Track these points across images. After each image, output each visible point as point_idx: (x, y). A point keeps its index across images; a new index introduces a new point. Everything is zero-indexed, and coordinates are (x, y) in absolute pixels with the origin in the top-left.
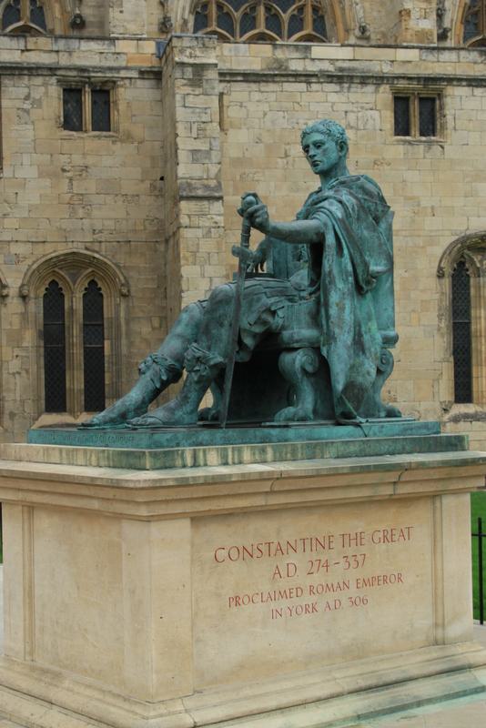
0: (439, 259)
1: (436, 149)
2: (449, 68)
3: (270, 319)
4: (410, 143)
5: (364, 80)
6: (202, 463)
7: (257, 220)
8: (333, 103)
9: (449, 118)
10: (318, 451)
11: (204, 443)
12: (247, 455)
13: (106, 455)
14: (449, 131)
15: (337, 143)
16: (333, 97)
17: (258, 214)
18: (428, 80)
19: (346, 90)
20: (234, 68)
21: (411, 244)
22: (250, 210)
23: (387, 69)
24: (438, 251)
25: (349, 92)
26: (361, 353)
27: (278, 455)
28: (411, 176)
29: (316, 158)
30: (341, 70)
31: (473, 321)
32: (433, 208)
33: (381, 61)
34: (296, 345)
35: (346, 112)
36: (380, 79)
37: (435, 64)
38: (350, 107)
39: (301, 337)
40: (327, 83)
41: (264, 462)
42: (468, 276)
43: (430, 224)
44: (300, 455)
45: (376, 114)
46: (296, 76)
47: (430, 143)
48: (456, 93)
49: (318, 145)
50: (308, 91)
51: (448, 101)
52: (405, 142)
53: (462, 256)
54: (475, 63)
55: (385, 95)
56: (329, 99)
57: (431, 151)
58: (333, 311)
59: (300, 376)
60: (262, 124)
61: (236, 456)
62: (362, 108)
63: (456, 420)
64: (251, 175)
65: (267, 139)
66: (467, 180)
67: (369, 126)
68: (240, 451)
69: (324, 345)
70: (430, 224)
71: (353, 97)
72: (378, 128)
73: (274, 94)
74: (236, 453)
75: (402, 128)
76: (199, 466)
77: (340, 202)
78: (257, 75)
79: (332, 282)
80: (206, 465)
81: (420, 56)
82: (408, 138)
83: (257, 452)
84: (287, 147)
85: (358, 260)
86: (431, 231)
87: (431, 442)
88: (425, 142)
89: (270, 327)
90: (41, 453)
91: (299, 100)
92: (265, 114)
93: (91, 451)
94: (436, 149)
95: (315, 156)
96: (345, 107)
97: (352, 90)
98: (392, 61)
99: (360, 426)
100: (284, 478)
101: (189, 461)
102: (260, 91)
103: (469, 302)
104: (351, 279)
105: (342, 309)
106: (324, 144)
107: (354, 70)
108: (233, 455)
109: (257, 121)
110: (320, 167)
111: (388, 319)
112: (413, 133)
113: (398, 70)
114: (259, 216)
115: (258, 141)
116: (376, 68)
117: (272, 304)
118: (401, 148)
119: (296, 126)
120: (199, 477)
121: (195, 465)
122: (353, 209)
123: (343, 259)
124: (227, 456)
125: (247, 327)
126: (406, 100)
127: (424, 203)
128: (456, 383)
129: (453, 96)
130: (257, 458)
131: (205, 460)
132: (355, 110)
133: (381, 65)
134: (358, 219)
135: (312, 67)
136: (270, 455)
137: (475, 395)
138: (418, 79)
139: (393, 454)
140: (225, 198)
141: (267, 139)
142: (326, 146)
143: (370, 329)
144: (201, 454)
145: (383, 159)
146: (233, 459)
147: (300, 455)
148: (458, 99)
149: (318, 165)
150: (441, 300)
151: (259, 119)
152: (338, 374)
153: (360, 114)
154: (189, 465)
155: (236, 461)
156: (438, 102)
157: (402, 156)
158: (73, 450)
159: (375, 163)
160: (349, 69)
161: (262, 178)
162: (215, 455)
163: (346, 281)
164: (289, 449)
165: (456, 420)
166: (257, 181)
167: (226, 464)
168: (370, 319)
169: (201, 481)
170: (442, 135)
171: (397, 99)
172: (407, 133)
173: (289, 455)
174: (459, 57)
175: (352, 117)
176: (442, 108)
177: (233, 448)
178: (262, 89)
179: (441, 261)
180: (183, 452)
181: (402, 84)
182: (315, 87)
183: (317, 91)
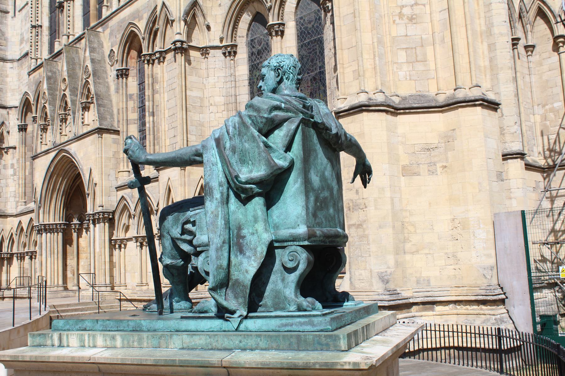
6: (65, 345)
10: (162, 341)
11: (88, 329)
12: (100, 341)
26: (238, 254)
27: (126, 342)
39: (200, 242)
44: (145, 344)
61: (91, 341)
68: (94, 337)
74: (91, 338)
76: (63, 346)
80: (68, 346)
83: (108, 339)
87: (292, 340)
101: (56, 343)
108: (89, 340)
111: (298, 218)
117: (191, 217)
120: (26, 356)
121: (60, 346)
122: (234, 127)
124: (85, 340)
125: (179, 236)
130: (108, 343)
131: (68, 342)
134: (239, 135)
136: (119, 343)
139: (244, 349)
143: (257, 230)
144: (64, 338)
146: (89, 342)
147: (145, 344)
154: (56, 345)
155: (91, 345)
162: (75, 339)
164: (136, 338)
168: (256, 220)
169: (28, 359)
173: (136, 344)
177: (89, 334)
180: (52, 336)
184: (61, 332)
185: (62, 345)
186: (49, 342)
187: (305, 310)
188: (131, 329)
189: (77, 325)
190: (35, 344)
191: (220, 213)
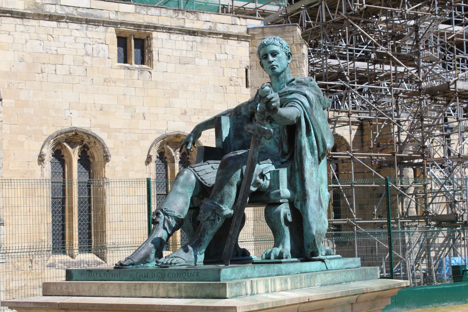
0: (148, 150)
2: (154, 19)
3: (261, 181)
4: (128, 68)
7: (273, 104)
8: (76, 37)
9: (155, 53)
13: (177, 287)
14: (154, 62)
15: (286, 54)
17: (273, 100)
20: (4, 6)
22: (269, 97)
23: (113, 17)
24: (148, 144)
29: (273, 63)
33: (109, 10)
34: (281, 201)
36: (107, 23)
37: (146, 16)
40: (71, 22)
41: (286, 290)
46: (50, 17)
47: (142, 70)
48: (159, 37)
49: (274, 54)
50: (58, 27)
51: (154, 41)
53: (163, 148)
55: (111, 35)
56: (73, 34)
57: (143, 75)
58: (307, 175)
59: (283, 224)
60: (24, 48)
62: (96, 42)
64: (16, 85)
65: (28, 59)
67: (101, 54)
68: (274, 281)
69: (298, 201)
71: (90, 34)
73: (33, 28)
75: (125, 58)
76: (254, 294)
77: (305, 95)
78: (18, 13)
79: (305, 154)
81: (136, 9)
82: (126, 65)
83: (283, 283)
84: (43, 66)
85: (320, 139)
86: (143, 130)
88: (138, 68)
89: (261, 187)
91: (51, 34)
92: (27, 41)
95: (272, 61)
96: (84, 41)
97: (89, 29)
98: (117, 12)
99: (324, 262)
100: (311, 301)
102: (23, 25)
104: (316, 152)
105: (312, 174)
106: (279, 53)
107: (92, 15)
108: (271, 285)
109: (21, 46)
110: (278, 70)
113: (120, 18)
114: (274, 102)
115: (22, 60)
116: (105, 15)
119: (49, 52)
121: (252, 294)
123: (310, 137)
126: (125, 39)
127: (138, 111)
131: (257, 289)
132: (91, 43)
133: (109, 14)
134: (315, 109)
140: (3, 100)
141: (28, 59)
142: (280, 55)
144: (255, 284)
145: (110, 78)
151: (22, 44)
153: (94, 46)
154: (249, 294)
156: (146, 41)
158: (135, 285)
160: (87, 14)
161: (24, 88)
163: (312, 153)
164: (299, 280)
166: (20, 89)
167: (267, 292)
169: (270, 306)
170: (151, 65)
171: (118, 38)
172: (125, 61)
174: (161, 12)
175: (89, 48)
176: (150, 46)
178: (25, 23)
179: (149, 151)
180: (246, 284)
181: (123, 28)
182: (63, 25)
183: (64, 28)
184: (252, 279)
185: (253, 293)
186: (244, 292)
187: (330, 255)
188: (276, 274)
189: (241, 272)
190: (233, 295)
191: (314, 172)
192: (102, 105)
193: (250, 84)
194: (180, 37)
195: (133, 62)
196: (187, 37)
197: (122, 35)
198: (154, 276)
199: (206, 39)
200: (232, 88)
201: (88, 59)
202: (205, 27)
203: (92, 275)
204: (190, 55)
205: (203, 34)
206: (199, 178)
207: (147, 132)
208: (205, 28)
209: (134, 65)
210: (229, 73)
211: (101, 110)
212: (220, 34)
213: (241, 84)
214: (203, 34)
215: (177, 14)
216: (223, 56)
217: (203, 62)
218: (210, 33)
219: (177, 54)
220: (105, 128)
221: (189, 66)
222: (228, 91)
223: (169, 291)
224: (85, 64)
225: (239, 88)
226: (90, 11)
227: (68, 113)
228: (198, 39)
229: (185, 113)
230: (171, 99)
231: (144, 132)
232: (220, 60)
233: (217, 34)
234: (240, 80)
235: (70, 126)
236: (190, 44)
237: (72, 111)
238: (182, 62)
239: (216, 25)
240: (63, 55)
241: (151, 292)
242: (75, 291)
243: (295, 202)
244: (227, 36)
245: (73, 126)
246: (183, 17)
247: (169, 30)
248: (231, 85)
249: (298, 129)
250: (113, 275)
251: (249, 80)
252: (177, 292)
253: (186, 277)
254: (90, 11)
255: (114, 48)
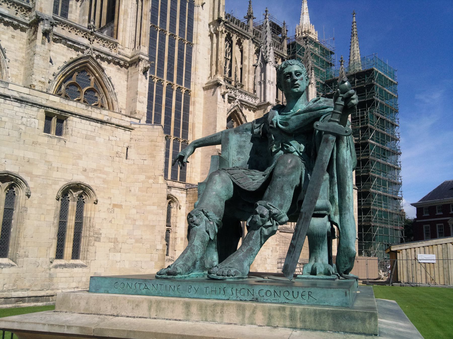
1: (62, 142)
2: (72, 109)
4: (51, 137)
5: (34, 104)
13: (288, 313)
16: (16, 109)
18: (62, 111)
19: (23, 107)
21: (45, 183)
23: (44, 103)
25: (25, 108)
28: (49, 152)
29: (297, 82)
30: (22, 97)
31: (69, 221)
32: (58, 168)
35: (22, 117)
38: (24, 115)
42: (69, 201)
43: (56, 175)
45: (36, 121)
51: (69, 122)
52: (49, 136)
54: (83, 109)
55: (41, 113)
62: (30, 117)
63: (56, 267)
66: (75, 158)
67: (33, 126)
69: (335, 214)
70: (56, 175)
71: (26, 111)
72: (37, 127)
86: (56, 178)
90: (145, 306)
93: (255, 308)
94: (62, 142)
95: (297, 80)
96: (21, 115)
97: (26, 108)
103: (68, 212)
106: (301, 74)
107: (29, 99)
112: (52, 133)
114: (353, 99)
116: (39, 101)
118: (46, 139)
128: (57, 249)
129: (72, 121)
132: (27, 117)
135: (7, 93)
137: (65, 255)
138: (58, 110)
148: (75, 123)
149: (298, 87)
150: (56, 210)
152: (352, 238)
153: (29, 119)
157: (46, 142)
159: (33, 143)
165: (56, 267)
175: (24, 120)
182: (8, 102)
192: (29, 158)
193: (128, 157)
194: (88, 122)
195: (54, 133)
196: (92, 123)
197: (49, 115)
198: (234, 292)
199: (104, 126)
200: (118, 159)
201: (23, 127)
202: (105, 119)
203: (133, 287)
204: (93, 134)
205: (102, 122)
206: (234, 181)
207: (58, 180)
208: (105, 119)
209: (55, 136)
210: (117, 149)
211: (28, 162)
212: (114, 124)
213: (123, 157)
214: (102, 122)
215: (87, 108)
216: (114, 138)
217: (100, 140)
218: (106, 123)
219: (84, 132)
220: (29, 174)
221: (92, 141)
222: (114, 160)
223: (272, 317)
224: (21, 130)
225: (121, 159)
226: (28, 96)
227: (3, 161)
228: (99, 125)
229: (85, 170)
230: (77, 160)
231: (57, 179)
232: (112, 140)
233: (112, 124)
234: (122, 154)
235: (4, 170)
236: (94, 127)
237: (7, 160)
238: (87, 138)
239: (111, 119)
240: (6, 122)
241: (241, 317)
242: (109, 308)
243: (332, 216)
244: (118, 126)
245: (7, 170)
246: (91, 110)
247: (81, 117)
248: (117, 156)
249: (341, 140)
250: (168, 288)
251: (128, 155)
252: (288, 320)
253: (290, 297)
254: (28, 96)
255: (42, 123)
